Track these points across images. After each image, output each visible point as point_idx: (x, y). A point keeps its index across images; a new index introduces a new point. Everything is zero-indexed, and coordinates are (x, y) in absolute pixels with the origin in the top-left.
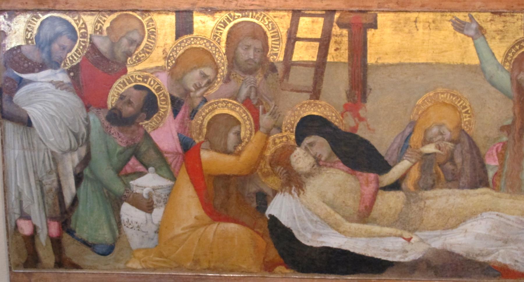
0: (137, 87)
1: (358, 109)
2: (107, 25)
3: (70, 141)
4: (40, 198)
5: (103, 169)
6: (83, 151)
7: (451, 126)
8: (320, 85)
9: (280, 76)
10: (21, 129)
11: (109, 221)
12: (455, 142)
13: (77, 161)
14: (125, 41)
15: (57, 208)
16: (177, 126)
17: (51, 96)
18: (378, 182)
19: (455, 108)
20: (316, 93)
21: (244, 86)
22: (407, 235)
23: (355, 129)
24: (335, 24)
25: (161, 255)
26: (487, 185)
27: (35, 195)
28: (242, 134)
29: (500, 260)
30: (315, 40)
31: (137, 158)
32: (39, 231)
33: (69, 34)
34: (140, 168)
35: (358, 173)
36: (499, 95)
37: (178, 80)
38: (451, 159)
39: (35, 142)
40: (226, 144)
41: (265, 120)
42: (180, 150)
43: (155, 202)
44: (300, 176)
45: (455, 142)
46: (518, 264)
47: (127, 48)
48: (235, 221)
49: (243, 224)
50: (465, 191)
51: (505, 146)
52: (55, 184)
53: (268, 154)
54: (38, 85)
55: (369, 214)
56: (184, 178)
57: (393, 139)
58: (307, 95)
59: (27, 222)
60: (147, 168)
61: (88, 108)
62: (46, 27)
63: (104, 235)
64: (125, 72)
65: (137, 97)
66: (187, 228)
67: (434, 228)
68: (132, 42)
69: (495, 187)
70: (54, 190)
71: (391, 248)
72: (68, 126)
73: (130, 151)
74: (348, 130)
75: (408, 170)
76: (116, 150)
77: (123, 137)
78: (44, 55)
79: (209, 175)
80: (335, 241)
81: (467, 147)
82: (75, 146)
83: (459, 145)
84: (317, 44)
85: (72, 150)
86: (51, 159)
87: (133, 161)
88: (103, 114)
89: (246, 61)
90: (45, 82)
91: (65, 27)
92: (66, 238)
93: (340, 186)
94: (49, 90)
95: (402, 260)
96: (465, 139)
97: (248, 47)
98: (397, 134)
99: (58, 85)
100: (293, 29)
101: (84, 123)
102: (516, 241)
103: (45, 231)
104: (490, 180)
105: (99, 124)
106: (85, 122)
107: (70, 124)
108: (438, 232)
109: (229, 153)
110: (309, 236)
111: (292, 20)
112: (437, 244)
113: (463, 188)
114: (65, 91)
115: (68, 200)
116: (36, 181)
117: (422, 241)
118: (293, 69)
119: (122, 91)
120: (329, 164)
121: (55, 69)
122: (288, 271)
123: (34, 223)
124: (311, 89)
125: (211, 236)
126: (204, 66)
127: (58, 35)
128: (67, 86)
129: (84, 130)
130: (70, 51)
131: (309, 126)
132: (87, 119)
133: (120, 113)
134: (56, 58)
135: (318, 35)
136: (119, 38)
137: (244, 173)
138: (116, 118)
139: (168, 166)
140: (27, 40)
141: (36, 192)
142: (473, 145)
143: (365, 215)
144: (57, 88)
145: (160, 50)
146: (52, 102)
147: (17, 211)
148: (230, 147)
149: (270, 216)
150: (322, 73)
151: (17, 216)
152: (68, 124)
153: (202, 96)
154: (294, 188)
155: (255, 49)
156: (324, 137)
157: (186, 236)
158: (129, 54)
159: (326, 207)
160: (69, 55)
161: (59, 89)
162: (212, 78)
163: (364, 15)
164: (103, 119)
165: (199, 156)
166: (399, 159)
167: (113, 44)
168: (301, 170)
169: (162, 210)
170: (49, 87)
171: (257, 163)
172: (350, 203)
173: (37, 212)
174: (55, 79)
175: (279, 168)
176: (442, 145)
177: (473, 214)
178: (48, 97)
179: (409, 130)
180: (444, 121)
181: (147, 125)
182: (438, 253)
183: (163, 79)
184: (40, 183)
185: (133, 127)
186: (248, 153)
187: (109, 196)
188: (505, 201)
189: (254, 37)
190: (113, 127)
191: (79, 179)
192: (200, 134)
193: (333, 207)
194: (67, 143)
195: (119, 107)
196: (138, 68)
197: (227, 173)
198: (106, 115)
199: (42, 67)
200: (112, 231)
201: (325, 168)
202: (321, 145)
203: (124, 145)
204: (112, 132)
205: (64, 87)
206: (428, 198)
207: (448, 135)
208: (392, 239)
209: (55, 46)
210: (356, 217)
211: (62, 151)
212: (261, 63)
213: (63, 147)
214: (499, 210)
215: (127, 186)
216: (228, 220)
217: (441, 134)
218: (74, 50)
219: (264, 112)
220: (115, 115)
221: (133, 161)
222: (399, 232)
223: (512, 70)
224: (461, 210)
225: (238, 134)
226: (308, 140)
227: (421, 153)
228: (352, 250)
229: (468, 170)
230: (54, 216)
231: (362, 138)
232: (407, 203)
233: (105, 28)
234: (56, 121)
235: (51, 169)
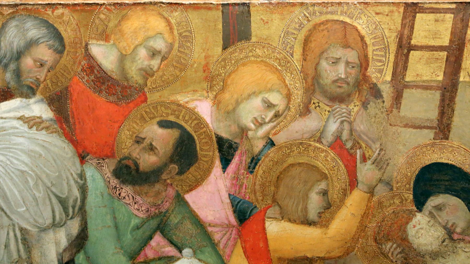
3: (53, 212)
6: (74, 227)
8: (450, 118)
9: (388, 103)
13: (64, 243)
14: (143, 52)
16: (228, 184)
17: (21, 140)
20: (443, 129)
21: (331, 120)
30: (441, 48)
31: (164, 235)
33: (51, 42)
37: (228, 113)
40: (305, 209)
41: (366, 172)
42: (233, 220)
44: (423, 256)
47: (146, 63)
58: (430, 134)
60: (180, 250)
61: (82, 159)
65: (163, 139)
72: (49, 188)
73: (154, 223)
76: (130, 222)
77: (141, 202)
78: (8, 76)
79: (280, 259)
82: (61, 219)
84: (444, 54)
85: (55, 225)
86: (20, 241)
87: (158, 239)
88: (109, 167)
89: (335, 81)
90: (10, 118)
91: (44, 31)
94: (16, 131)
97: (336, 62)
99: (32, 123)
100: (406, 32)
101: (76, 182)
105: (101, 184)
106: (79, 180)
107: (53, 185)
109: (310, 223)
111: (404, 18)
114: (44, 132)
118: (407, 93)
121: (27, 96)
124: (435, 124)
126: (270, 90)
127: (31, 44)
128: (48, 124)
129: (76, 193)
132: (82, 176)
133: (137, 165)
134: (28, 80)
136: (132, 47)
137: (336, 253)
138: (129, 174)
139: (214, 246)
144: (31, 128)
146: (22, 151)
148: (312, 215)
150: (452, 99)
152: (50, 185)
155: (347, 63)
156: (459, 198)
161: (35, 128)
162: (281, 107)
164: (109, 175)
165: (264, 229)
167: (122, 58)
168: (424, 248)
170: (18, 126)
171: (355, 239)
174: (27, 114)
175: (390, 244)
178: (14, 142)
185: (158, 187)
189: (346, 46)
190: (124, 187)
194: (48, 214)
195: (135, 155)
197: (309, 255)
198: (112, 168)
201: (462, 244)
203: (142, 215)
204: (123, 195)
205: (43, 125)
209: (28, 62)
211: (39, 227)
212: (358, 85)
213: (41, 221)
219: (364, 159)
220: (127, 167)
221: (158, 239)
226: (433, 202)
234: (29, 179)
235: (20, 256)
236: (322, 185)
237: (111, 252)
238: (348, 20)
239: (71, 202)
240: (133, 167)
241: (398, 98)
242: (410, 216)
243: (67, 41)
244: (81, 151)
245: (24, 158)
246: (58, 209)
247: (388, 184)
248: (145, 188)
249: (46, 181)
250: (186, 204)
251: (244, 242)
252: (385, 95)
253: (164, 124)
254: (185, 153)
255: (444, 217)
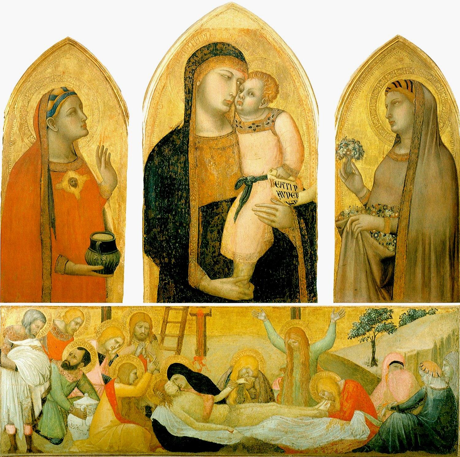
0: (80, 349)
1: (201, 359)
2: (63, 314)
4: (20, 412)
5: (58, 395)
6: (47, 385)
7: (253, 369)
9: (159, 342)
10: (11, 373)
11: (61, 424)
12: (256, 377)
13: (43, 391)
14: (73, 323)
15: (30, 418)
17: (30, 354)
18: (213, 400)
19: (255, 358)
20: (178, 351)
22: (231, 429)
23: (201, 370)
24: (188, 314)
25: (91, 444)
26: (274, 401)
27: (17, 411)
28: (138, 374)
29: (284, 443)
30: (178, 322)
32: (18, 432)
34: (80, 394)
35: (202, 395)
36: (279, 351)
38: (254, 387)
39: (19, 380)
41: (151, 366)
43: (88, 413)
44: (170, 396)
45: (256, 377)
46: (294, 445)
47: (74, 327)
48: (134, 423)
49: (138, 424)
50: (262, 404)
51: (283, 380)
52: (30, 404)
53: (152, 385)
54: (22, 347)
55: (209, 418)
56: (105, 399)
57: (221, 376)
59: (12, 426)
61: (51, 360)
62: (28, 315)
63: (57, 433)
64: (73, 339)
65: (80, 354)
66: (106, 427)
67: (246, 425)
68: (77, 324)
69: (278, 402)
70: (29, 407)
71: (222, 437)
73: (75, 384)
74: (197, 371)
75: (230, 393)
79: (119, 397)
80: (191, 433)
81: (262, 379)
83: (257, 379)
88: (60, 363)
92: (35, 435)
93: (192, 402)
95: (228, 444)
96: (260, 375)
98: (223, 373)
102: (292, 432)
103: (22, 432)
104: (276, 398)
108: (248, 428)
110: (176, 430)
112: (248, 434)
113: (261, 402)
115: (37, 413)
116: (18, 403)
117: (239, 432)
118: (166, 338)
119: (71, 350)
120: (186, 390)
122: (164, 451)
123: (16, 427)
125: (119, 432)
129: (48, 373)
130: (41, 328)
131: (175, 369)
132: (50, 367)
135: (180, 320)
138: (67, 366)
139: (96, 392)
140: (17, 322)
141: (18, 409)
142: (265, 379)
143: (206, 419)
145: (93, 328)
147: (6, 420)
148: (131, 381)
149: (155, 420)
150: (182, 340)
151: (6, 423)
153: (116, 353)
154: (166, 403)
155: (145, 327)
157: (105, 432)
158: (75, 330)
159: (185, 413)
160: (41, 331)
163: (205, 309)
166: (225, 387)
167: (66, 325)
169: (92, 418)
172: (198, 411)
173: (18, 421)
174: (32, 344)
176: (248, 379)
177: (267, 418)
179: (230, 371)
180: (249, 366)
181: (84, 369)
182: (249, 439)
183: (94, 343)
184: (21, 404)
185: (76, 370)
186: (142, 384)
187: (61, 410)
188: (284, 409)
191: (44, 401)
192: (114, 374)
193: (189, 414)
195: (69, 359)
196: (80, 338)
197: (130, 396)
198: (61, 364)
199: (25, 338)
200: (62, 429)
201: (184, 392)
202: (181, 379)
206: (241, 408)
207: (251, 373)
208: (222, 431)
210: (201, 419)
212: (148, 335)
214: (281, 415)
215: (72, 404)
216: (129, 422)
217: (248, 373)
218: (44, 328)
219: (150, 361)
221: (76, 389)
222: (226, 428)
223: (285, 338)
224: (260, 415)
225: (136, 373)
226: (174, 377)
227: (236, 383)
228: (200, 438)
229: (263, 393)
230: (28, 423)
231: (204, 376)
232: (230, 412)
233: (62, 316)
236: (135, 371)
237: (59, 394)
238: (145, 312)
239: (46, 376)
240: (68, 363)
241: (163, 340)
242: (166, 382)
243: (47, 319)
244: (50, 358)
245: (30, 360)
246: (42, 378)
247: (159, 370)
248: (72, 371)
249: (38, 368)
250: (86, 377)
251: (107, 391)
252: (158, 339)
253: (80, 349)
254: (87, 359)
255: (178, 382)
